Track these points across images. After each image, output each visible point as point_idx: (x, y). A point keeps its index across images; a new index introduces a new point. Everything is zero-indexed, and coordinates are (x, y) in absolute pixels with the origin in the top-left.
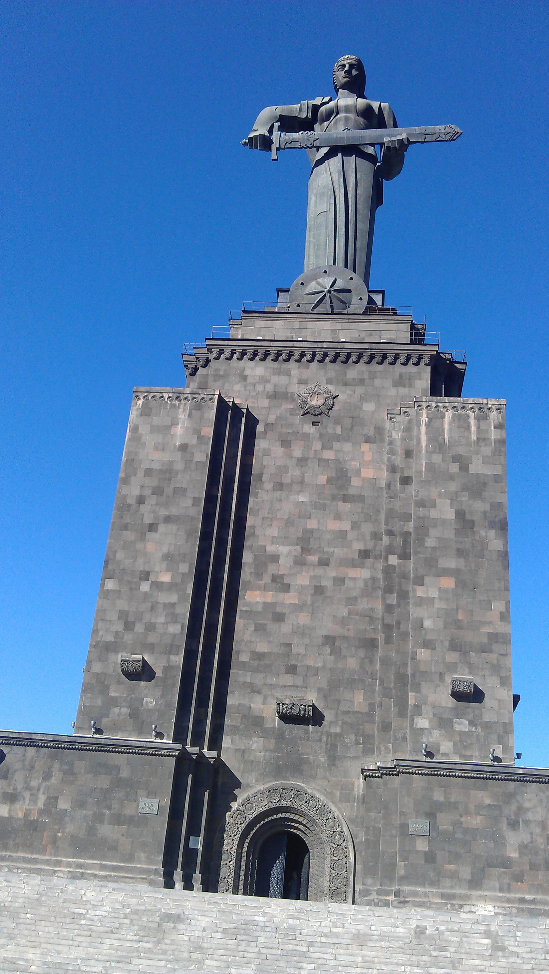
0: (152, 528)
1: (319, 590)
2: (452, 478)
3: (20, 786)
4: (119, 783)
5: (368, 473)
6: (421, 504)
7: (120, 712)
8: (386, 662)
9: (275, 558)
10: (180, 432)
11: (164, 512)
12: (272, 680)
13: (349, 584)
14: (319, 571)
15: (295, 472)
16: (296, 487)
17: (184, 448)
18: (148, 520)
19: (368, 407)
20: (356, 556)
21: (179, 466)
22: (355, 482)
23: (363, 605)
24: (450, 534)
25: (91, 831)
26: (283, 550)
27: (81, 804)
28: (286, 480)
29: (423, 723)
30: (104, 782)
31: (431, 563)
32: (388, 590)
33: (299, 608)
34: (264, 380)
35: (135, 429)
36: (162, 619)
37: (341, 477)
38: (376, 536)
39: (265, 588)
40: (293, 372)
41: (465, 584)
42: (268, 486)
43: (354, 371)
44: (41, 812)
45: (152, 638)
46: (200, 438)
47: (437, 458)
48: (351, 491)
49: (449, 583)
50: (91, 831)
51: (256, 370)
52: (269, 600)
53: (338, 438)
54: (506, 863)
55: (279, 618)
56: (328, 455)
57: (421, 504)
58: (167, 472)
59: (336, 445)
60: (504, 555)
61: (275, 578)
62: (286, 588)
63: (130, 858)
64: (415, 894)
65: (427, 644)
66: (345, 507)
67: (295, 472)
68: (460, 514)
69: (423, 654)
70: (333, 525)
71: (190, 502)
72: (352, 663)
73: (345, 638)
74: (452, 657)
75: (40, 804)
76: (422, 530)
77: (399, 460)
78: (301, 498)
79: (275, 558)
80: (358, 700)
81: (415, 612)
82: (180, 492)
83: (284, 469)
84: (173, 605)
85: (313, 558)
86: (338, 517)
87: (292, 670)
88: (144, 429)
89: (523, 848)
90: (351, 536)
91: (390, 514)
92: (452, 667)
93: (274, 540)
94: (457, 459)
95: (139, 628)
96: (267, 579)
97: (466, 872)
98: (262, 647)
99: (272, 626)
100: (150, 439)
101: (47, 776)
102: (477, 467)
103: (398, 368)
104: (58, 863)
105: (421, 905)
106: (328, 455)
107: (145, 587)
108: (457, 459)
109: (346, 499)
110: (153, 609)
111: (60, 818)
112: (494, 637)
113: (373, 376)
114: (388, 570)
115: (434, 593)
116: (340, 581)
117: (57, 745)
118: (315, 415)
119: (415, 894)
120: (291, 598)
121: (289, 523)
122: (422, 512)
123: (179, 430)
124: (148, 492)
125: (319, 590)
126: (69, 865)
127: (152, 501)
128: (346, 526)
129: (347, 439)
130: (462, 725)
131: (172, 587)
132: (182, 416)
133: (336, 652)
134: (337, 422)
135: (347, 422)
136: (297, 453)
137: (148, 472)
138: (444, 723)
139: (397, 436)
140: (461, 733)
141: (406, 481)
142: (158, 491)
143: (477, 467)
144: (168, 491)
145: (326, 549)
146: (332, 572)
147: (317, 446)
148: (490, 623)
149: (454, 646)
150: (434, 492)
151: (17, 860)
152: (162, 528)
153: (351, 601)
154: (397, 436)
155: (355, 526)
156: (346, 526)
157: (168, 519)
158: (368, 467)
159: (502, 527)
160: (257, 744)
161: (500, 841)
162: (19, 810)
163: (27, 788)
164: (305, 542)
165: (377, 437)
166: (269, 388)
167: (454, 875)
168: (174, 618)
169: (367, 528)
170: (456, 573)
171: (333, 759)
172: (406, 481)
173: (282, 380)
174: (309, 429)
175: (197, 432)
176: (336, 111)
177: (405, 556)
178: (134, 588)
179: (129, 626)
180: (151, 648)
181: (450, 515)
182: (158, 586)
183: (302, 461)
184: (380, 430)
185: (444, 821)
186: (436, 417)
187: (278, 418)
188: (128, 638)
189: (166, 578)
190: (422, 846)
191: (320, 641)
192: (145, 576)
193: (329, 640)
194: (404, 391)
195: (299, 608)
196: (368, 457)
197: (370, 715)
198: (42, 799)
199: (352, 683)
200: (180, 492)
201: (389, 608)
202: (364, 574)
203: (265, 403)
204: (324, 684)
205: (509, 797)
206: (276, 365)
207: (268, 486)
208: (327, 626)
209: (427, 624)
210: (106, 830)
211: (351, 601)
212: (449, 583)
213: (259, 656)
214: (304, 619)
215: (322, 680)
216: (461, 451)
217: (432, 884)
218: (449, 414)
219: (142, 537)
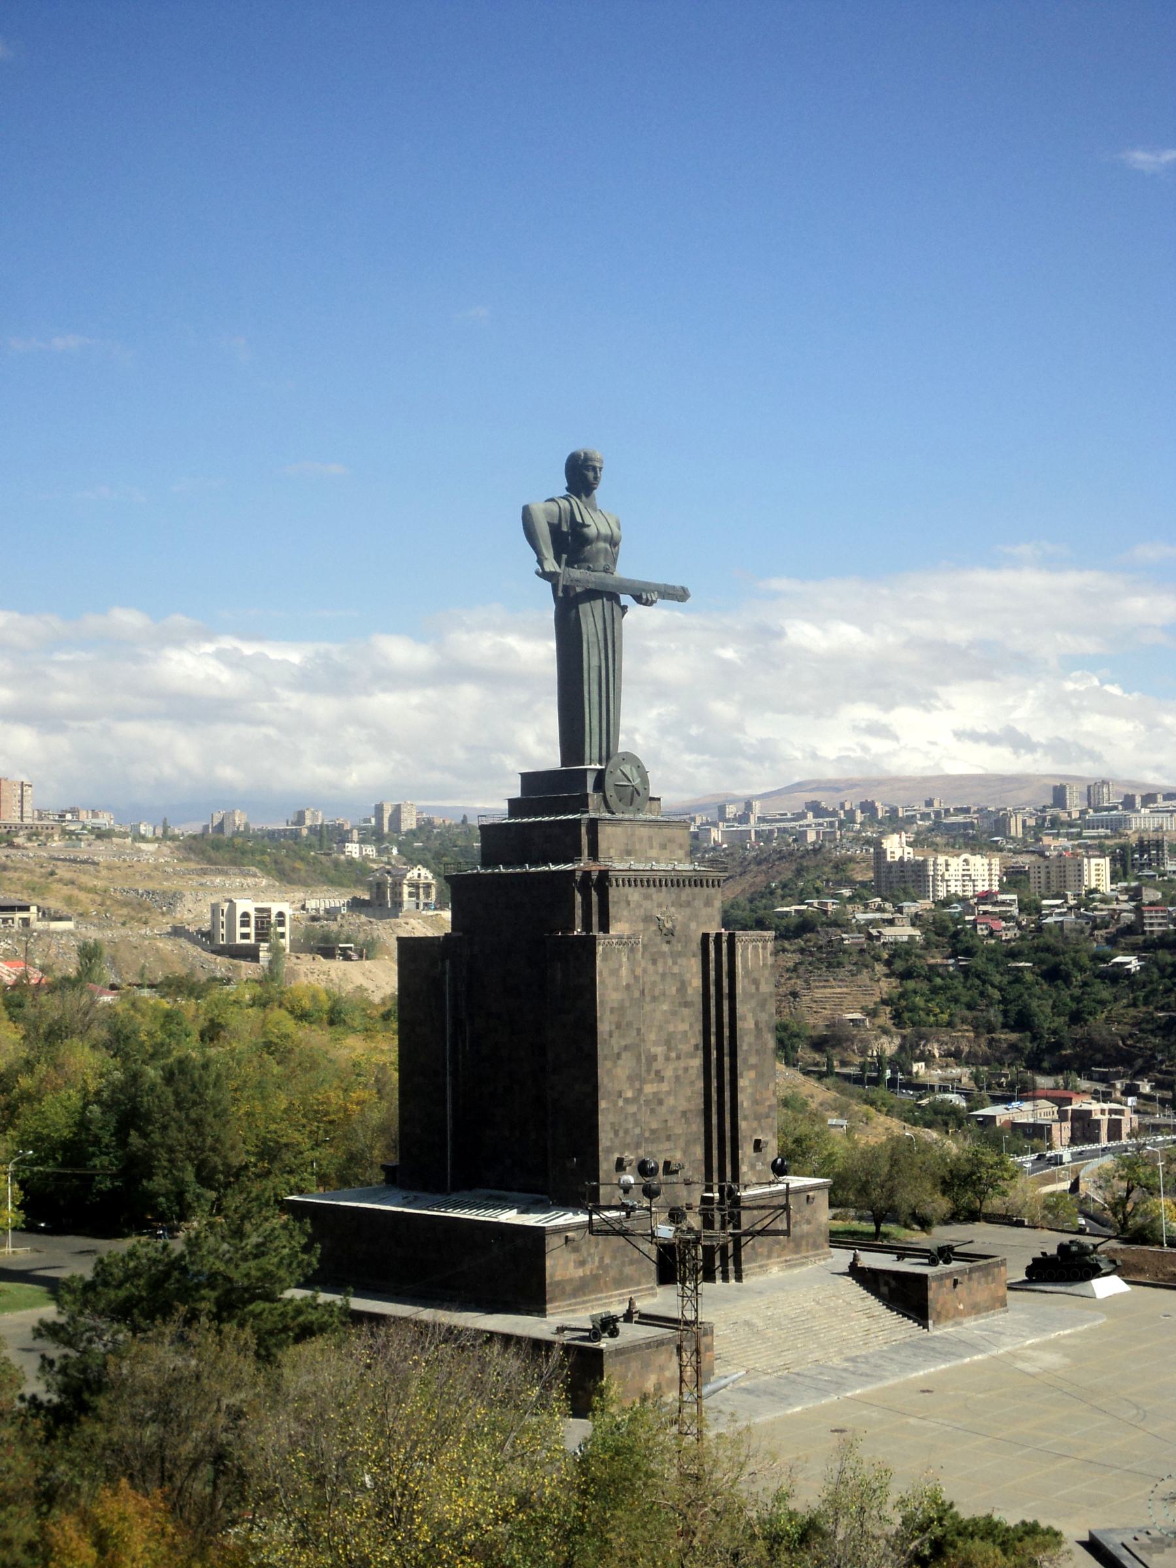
0: (619, 1056)
1: (677, 1078)
2: (752, 996)
3: (585, 1254)
9: (655, 1058)
11: (623, 1043)
12: (661, 1147)
13: (690, 1071)
14: (676, 1064)
16: (662, 998)
17: (628, 986)
18: (616, 1051)
20: (692, 1049)
21: (627, 1004)
22: (690, 991)
25: (621, 1272)
27: (614, 1258)
28: (657, 994)
31: (745, 1060)
33: (668, 1093)
34: (640, 906)
35: (601, 972)
36: (631, 1126)
37: (683, 987)
39: (652, 1082)
40: (654, 897)
42: (648, 999)
43: (687, 893)
44: (598, 1268)
45: (628, 1140)
46: (636, 978)
47: (746, 981)
48: (689, 999)
49: (752, 1074)
50: (621, 1272)
51: (634, 894)
52: (655, 1090)
53: (679, 954)
55: (660, 1102)
59: (679, 961)
61: (658, 1072)
62: (661, 1079)
63: (639, 1284)
64: (750, 1269)
65: (745, 1118)
66: (686, 1011)
68: (756, 1024)
71: (634, 1033)
73: (690, 1111)
74: (755, 1124)
75: (597, 1264)
78: (665, 1007)
79: (655, 1058)
81: (741, 1097)
82: (629, 1024)
84: (635, 1114)
85: (673, 1055)
86: (683, 1021)
87: (669, 1138)
88: (605, 974)
90: (690, 1034)
92: (755, 1131)
93: (656, 1043)
95: (621, 1134)
96: (653, 1075)
98: (654, 1126)
99: (658, 1109)
100: (610, 981)
101: (597, 1245)
104: (611, 1296)
105: (752, 1274)
106: (676, 970)
109: (686, 1004)
110: (626, 1118)
113: (694, 899)
116: (686, 1069)
119: (750, 1269)
120: (665, 1087)
123: (624, 972)
124: (613, 1027)
126: (615, 1296)
129: (685, 956)
132: (625, 959)
133: (687, 1121)
134: (679, 942)
135: (683, 939)
136: (661, 970)
137: (612, 1010)
138: (752, 1166)
140: (760, 1171)
142: (618, 1026)
144: (624, 1023)
145: (680, 1046)
147: (670, 962)
148: (768, 1099)
149: (758, 1117)
151: (592, 1301)
152: (624, 1055)
153: (692, 1083)
155: (691, 1026)
162: (587, 1270)
163: (589, 1255)
164: (668, 1043)
166: (640, 912)
167: (762, 1255)
168: (637, 1123)
169: (699, 1026)
173: (647, 904)
174: (665, 948)
175: (633, 971)
178: (615, 1104)
179: (616, 1133)
180: (626, 1146)
181: (752, 1026)
182: (627, 1100)
183: (663, 975)
186: (745, 949)
187: (650, 939)
188: (617, 1141)
189: (629, 1094)
191: (679, 1115)
193: (684, 1113)
194: (709, 910)
198: (597, 1259)
203: (641, 926)
204: (683, 1145)
206: (644, 890)
207: (648, 999)
208: (683, 1105)
209: (745, 1104)
210: (629, 1270)
212: (752, 1074)
213: (653, 1132)
216: (756, 975)
217: (755, 1261)
218: (750, 947)
219: (615, 1065)
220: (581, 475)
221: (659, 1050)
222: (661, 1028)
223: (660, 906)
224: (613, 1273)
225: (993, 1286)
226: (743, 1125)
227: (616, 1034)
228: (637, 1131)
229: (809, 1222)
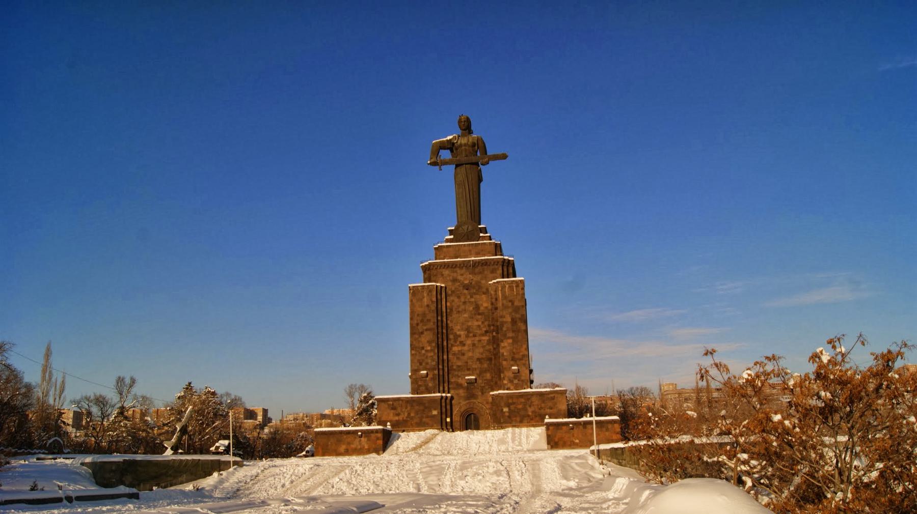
0: (422, 333)
1: (474, 345)
4: (426, 408)
5: (485, 305)
6: (501, 317)
7: (423, 388)
8: (495, 365)
10: (426, 301)
15: (462, 307)
17: (428, 306)
19: (483, 282)
22: (482, 308)
23: (488, 347)
24: (510, 325)
25: (421, 420)
26: (462, 333)
27: (417, 413)
29: (505, 382)
30: (422, 408)
31: (505, 335)
32: (494, 343)
33: (469, 351)
34: (449, 275)
37: (477, 307)
38: (489, 326)
41: (515, 341)
45: (428, 367)
47: (505, 302)
49: (510, 341)
50: (421, 420)
51: (446, 272)
53: (475, 294)
54: (529, 416)
55: (463, 354)
56: (473, 300)
57: (501, 317)
58: (424, 315)
60: (526, 331)
62: (464, 345)
65: (505, 360)
67: (462, 307)
68: (513, 319)
69: (504, 363)
70: (476, 323)
72: (486, 366)
74: (512, 363)
76: (503, 324)
77: (494, 300)
78: (466, 315)
79: (460, 336)
80: (488, 376)
81: (501, 351)
82: (429, 320)
83: (459, 306)
87: (469, 369)
89: (533, 412)
91: (493, 318)
94: (510, 301)
97: (518, 419)
98: (459, 364)
102: (516, 303)
103: (491, 267)
107: (423, 352)
108: (510, 301)
109: (479, 314)
111: (412, 418)
112: (523, 356)
114: (494, 337)
115: (506, 344)
116: (480, 341)
117: (408, 401)
118: (467, 287)
120: (466, 348)
121: (463, 324)
122: (501, 320)
123: (425, 299)
125: (474, 345)
127: (421, 324)
128: (480, 323)
130: (516, 381)
131: (431, 350)
133: (481, 363)
134: (474, 288)
136: (463, 300)
139: (492, 293)
141: (496, 309)
142: (422, 321)
143: (516, 303)
146: (477, 339)
149: (513, 359)
150: (504, 313)
153: (483, 347)
154: (492, 293)
156: (480, 323)
157: (426, 330)
158: (485, 303)
159: (525, 322)
160: (462, 392)
161: (526, 410)
162: (401, 418)
164: (468, 330)
165: (487, 292)
169: (486, 323)
170: (512, 338)
171: (482, 393)
172: (496, 309)
174: (466, 291)
176: (461, 145)
177: (497, 333)
179: (421, 364)
181: (509, 320)
182: (427, 351)
183: (464, 303)
184: (487, 289)
185: (512, 407)
189: (429, 348)
190: (507, 414)
192: (423, 348)
193: (478, 359)
195: (469, 351)
196: (485, 299)
197: (491, 380)
199: (486, 371)
200: (429, 320)
201: (494, 349)
202: (486, 338)
203: (450, 283)
205: (528, 399)
208: (477, 355)
211: (483, 347)
212: (510, 341)
213: (459, 366)
214: (470, 354)
215: (478, 372)
220: (466, 127)
221: (462, 333)
222: (463, 324)
223: (462, 275)
224: (416, 420)
225: (607, 433)
226: (504, 363)
227: (421, 324)
228: (434, 363)
229: (551, 408)
